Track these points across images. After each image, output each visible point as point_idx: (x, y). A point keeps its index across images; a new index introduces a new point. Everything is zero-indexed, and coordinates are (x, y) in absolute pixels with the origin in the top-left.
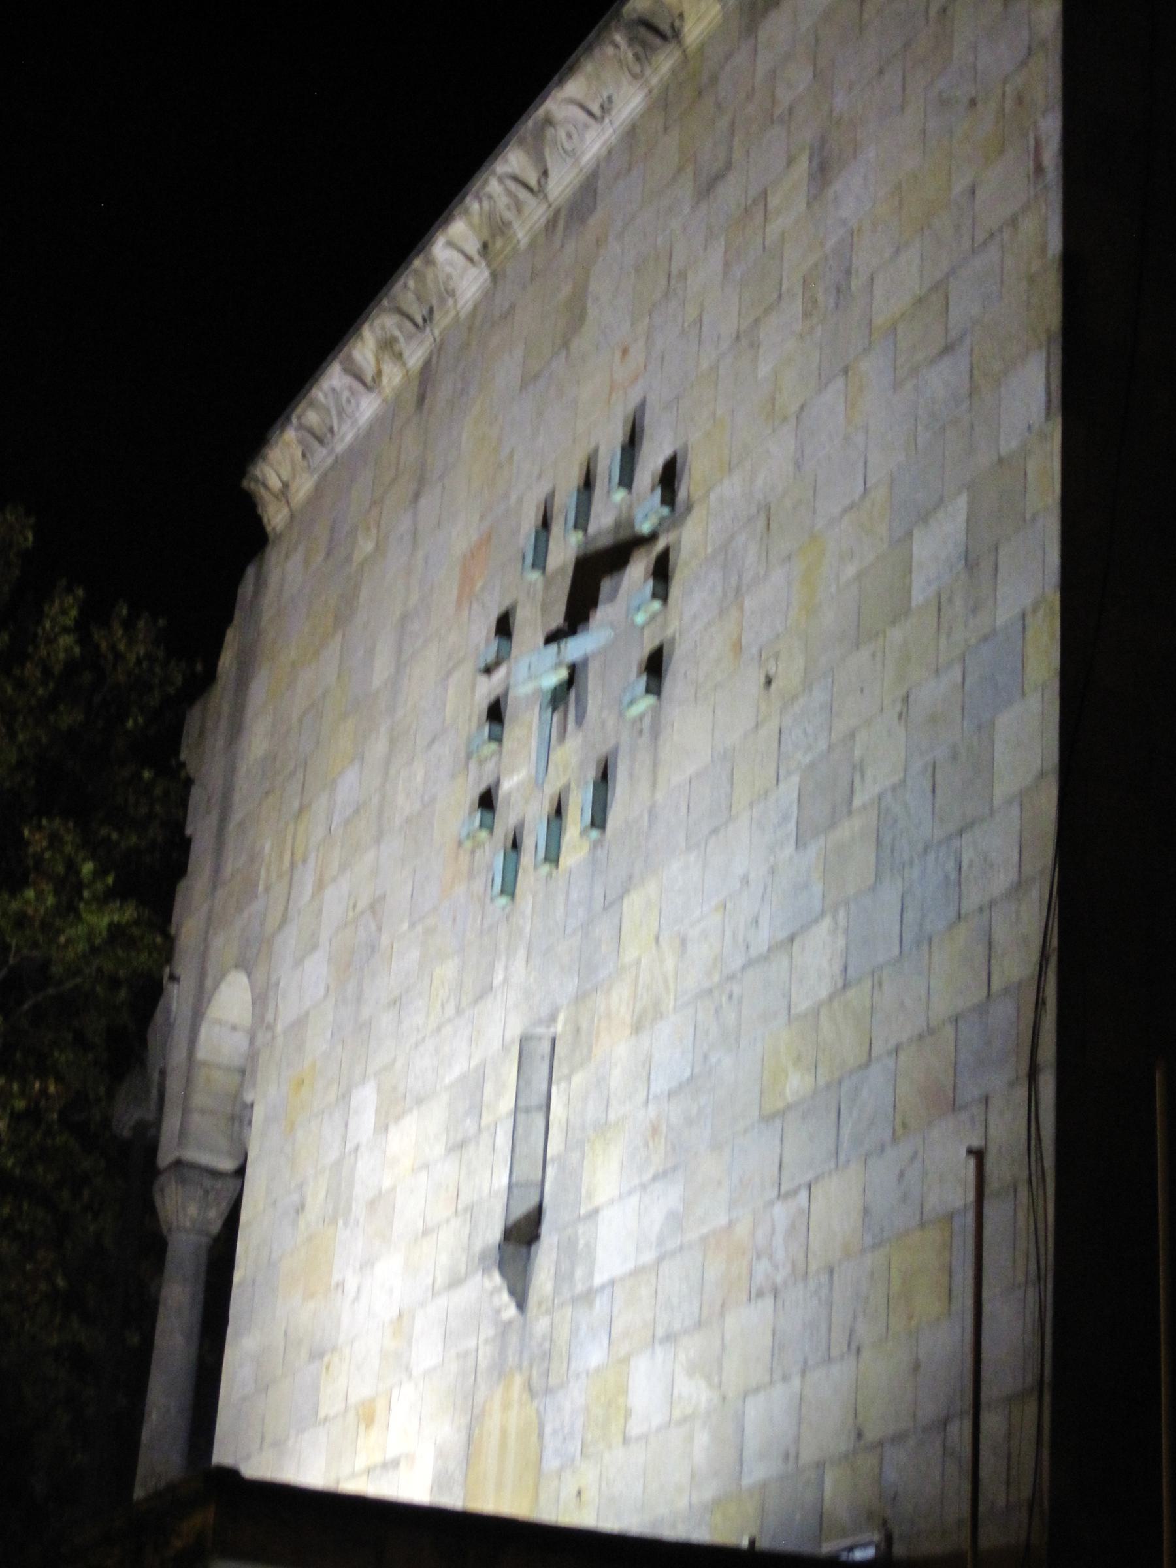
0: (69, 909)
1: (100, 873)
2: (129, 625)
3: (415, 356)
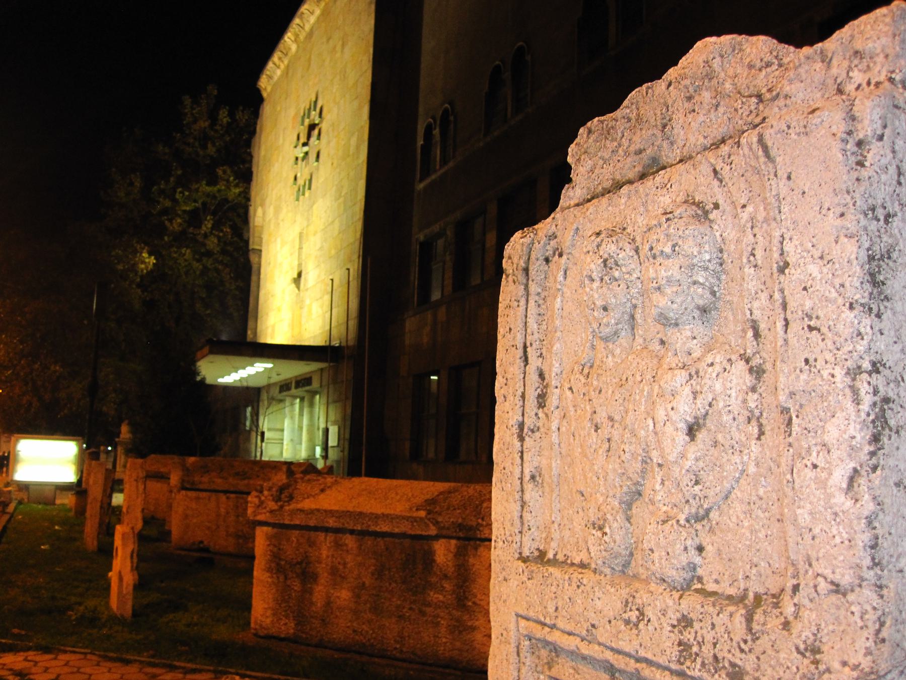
0: (228, 188)
1: (235, 180)
2: (243, 112)
3: (286, 62)
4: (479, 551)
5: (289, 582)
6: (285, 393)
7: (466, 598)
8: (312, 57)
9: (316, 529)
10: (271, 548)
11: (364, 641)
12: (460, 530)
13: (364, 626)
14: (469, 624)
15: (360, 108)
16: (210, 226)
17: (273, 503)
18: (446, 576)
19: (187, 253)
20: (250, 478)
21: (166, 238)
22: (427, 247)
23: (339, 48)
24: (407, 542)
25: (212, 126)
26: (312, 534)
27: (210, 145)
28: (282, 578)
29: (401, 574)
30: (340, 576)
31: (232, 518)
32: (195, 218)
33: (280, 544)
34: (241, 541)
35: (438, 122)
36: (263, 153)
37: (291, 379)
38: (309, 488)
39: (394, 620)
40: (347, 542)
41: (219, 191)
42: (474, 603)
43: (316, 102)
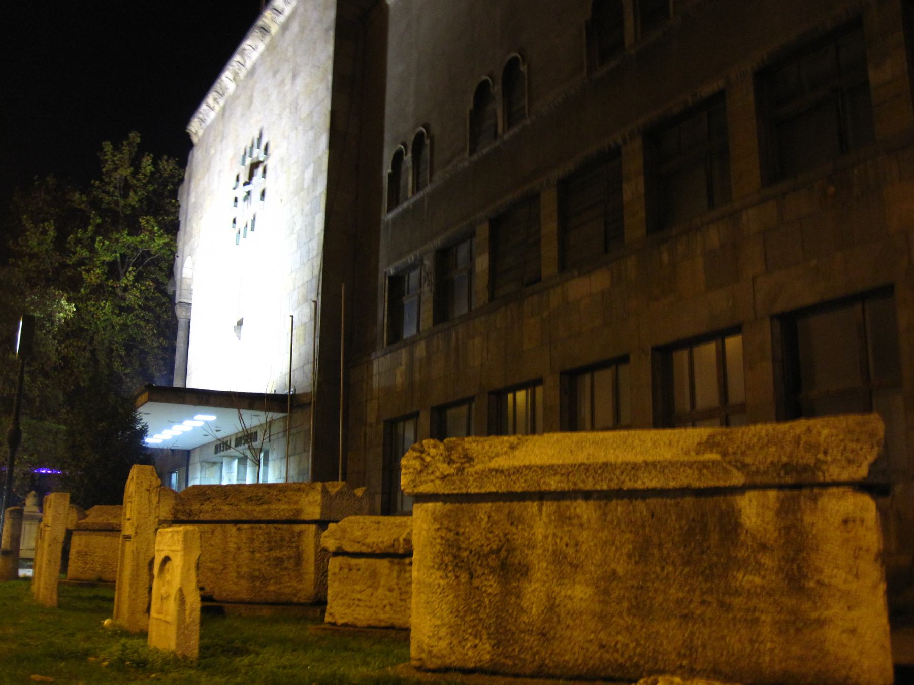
1: (159, 230)
2: (167, 161)
3: (222, 102)
4: (819, 503)
5: (476, 582)
6: (222, 453)
7: (805, 577)
8: (255, 94)
9: (523, 496)
10: (443, 533)
11: (621, 660)
12: (786, 473)
13: (620, 638)
14: (814, 615)
15: (316, 139)
16: (131, 278)
17: (445, 465)
18: (763, 547)
19: (108, 306)
20: (269, 503)
21: (82, 291)
22: (397, 282)
23: (288, 81)
24: (688, 502)
25: (134, 174)
26: (516, 506)
27: (131, 194)
28: (464, 577)
29: (681, 550)
30: (571, 564)
31: (246, 554)
32: (113, 270)
33: (458, 526)
34: (258, 584)
35: (410, 147)
36: (193, 199)
37: (230, 436)
38: (487, 447)
39: (674, 622)
40: (578, 511)
41: (142, 242)
42: (818, 582)
43: (260, 139)
